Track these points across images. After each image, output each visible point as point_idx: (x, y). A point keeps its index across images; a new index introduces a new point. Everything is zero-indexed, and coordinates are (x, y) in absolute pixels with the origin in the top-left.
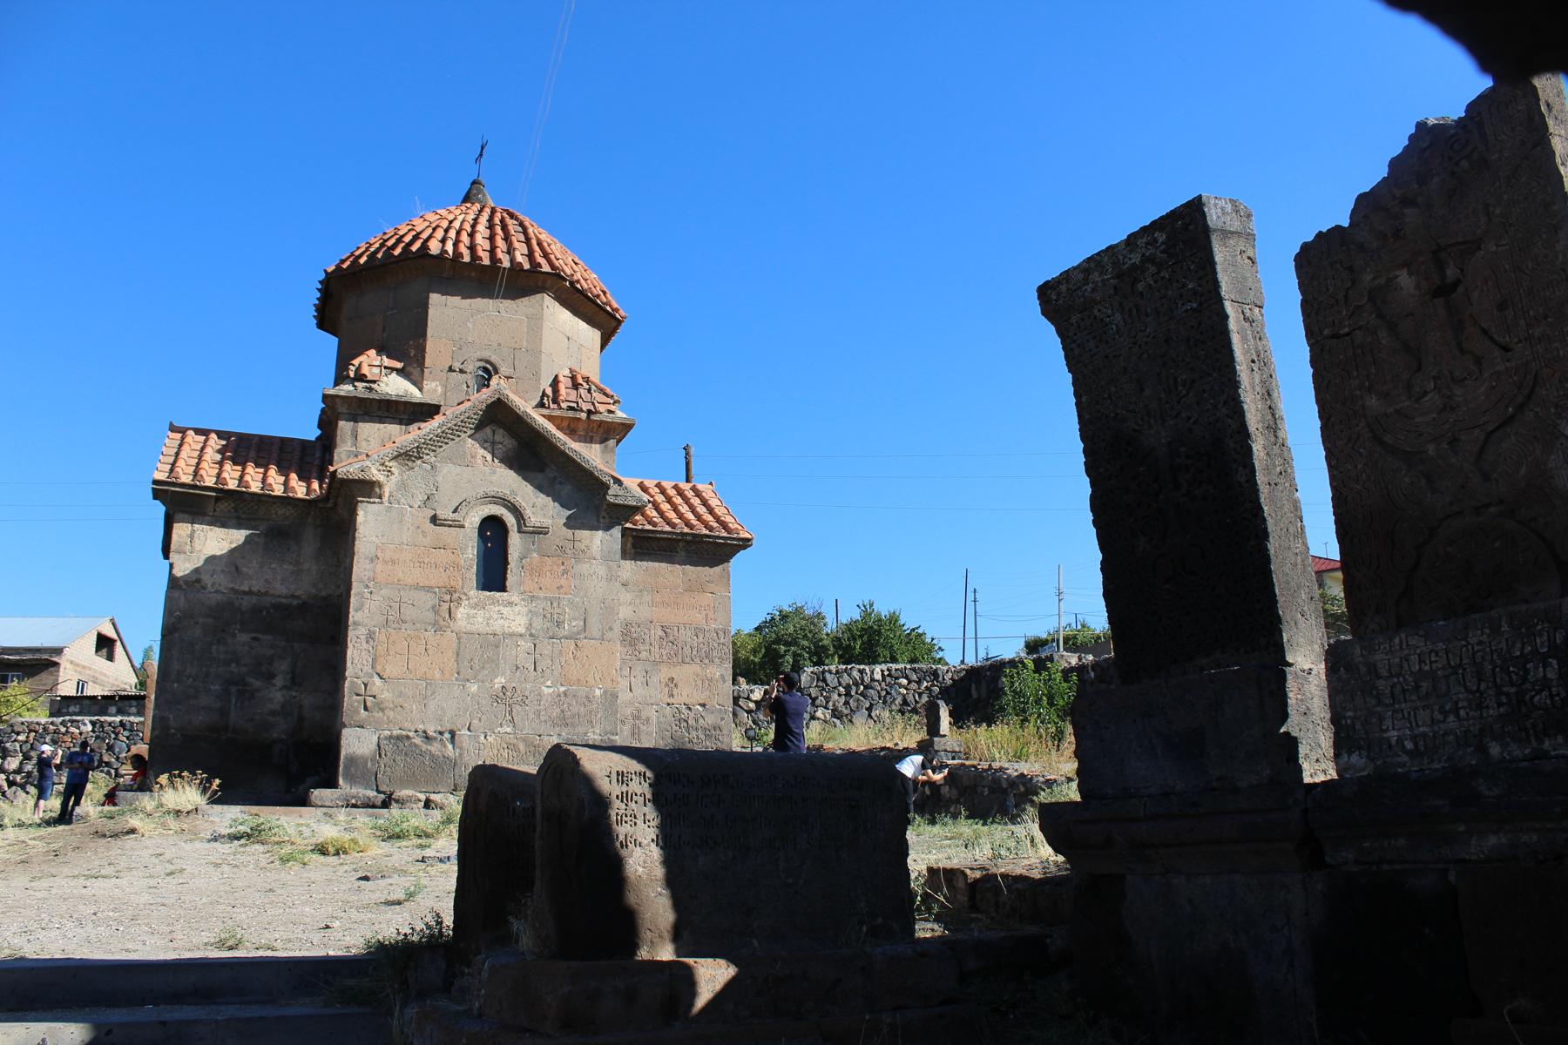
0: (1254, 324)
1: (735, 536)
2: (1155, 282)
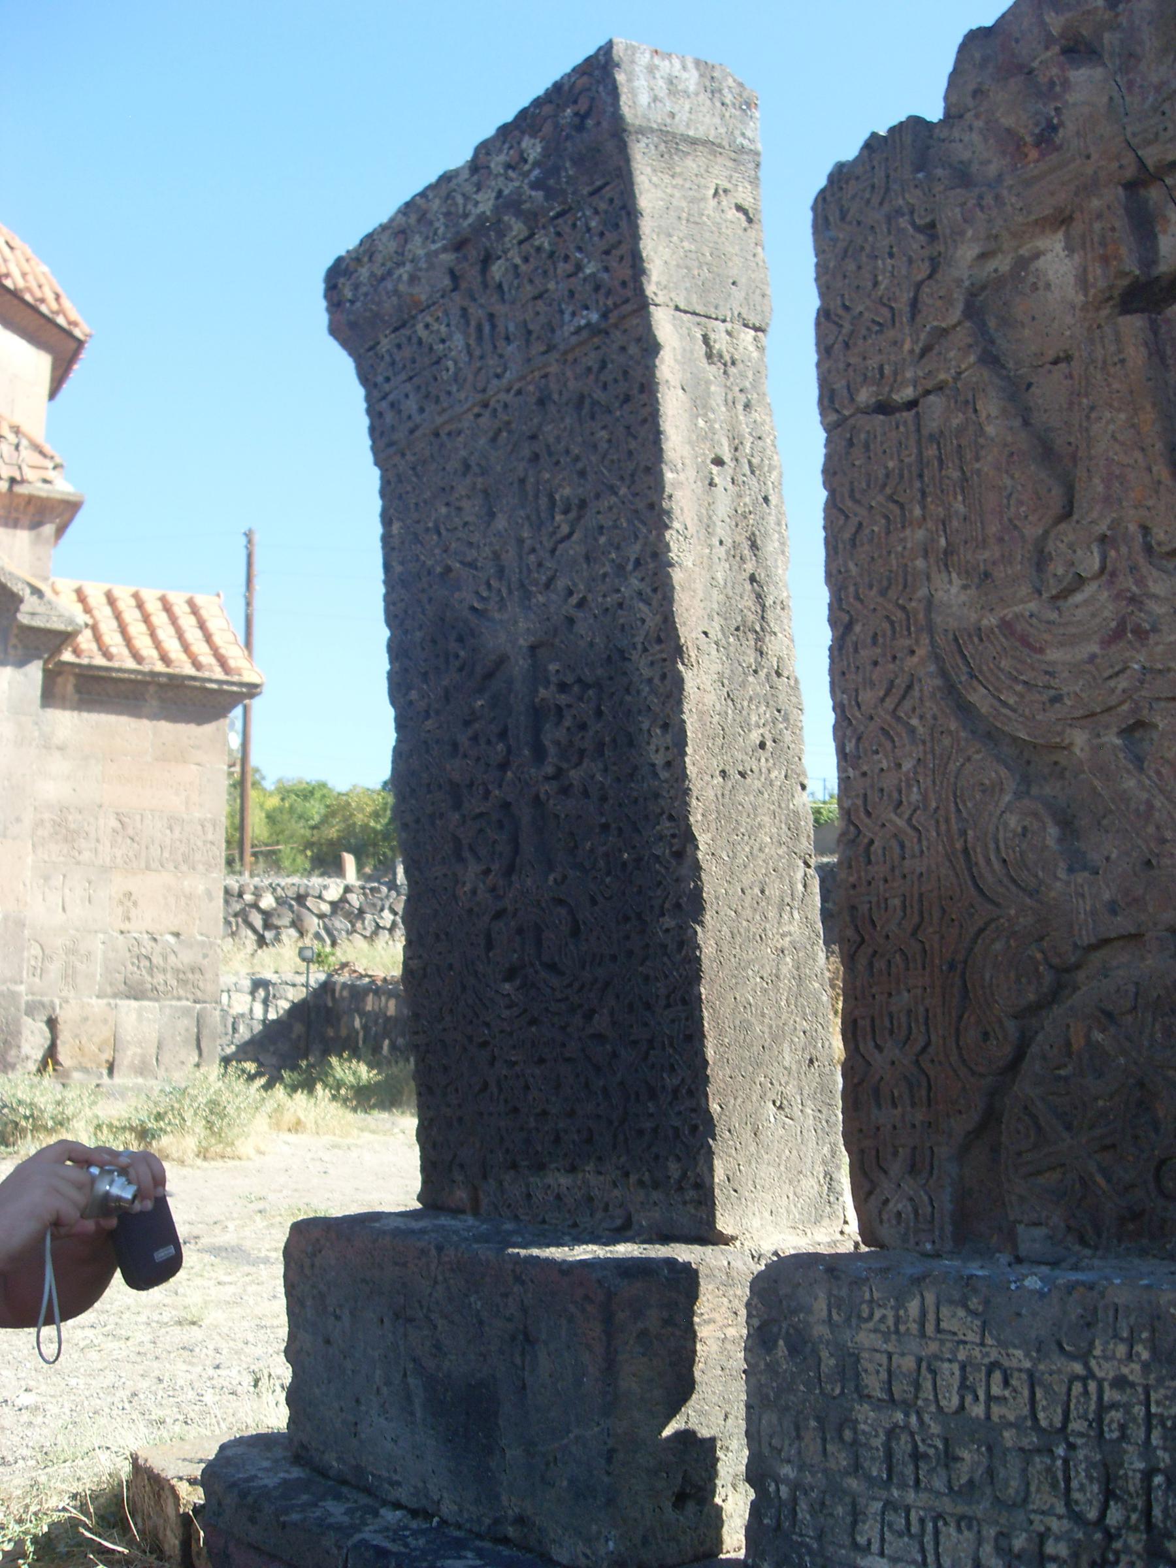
0: (732, 370)
1: (235, 678)
2: (526, 260)
